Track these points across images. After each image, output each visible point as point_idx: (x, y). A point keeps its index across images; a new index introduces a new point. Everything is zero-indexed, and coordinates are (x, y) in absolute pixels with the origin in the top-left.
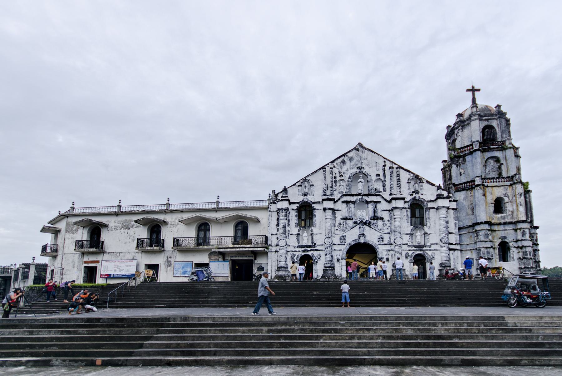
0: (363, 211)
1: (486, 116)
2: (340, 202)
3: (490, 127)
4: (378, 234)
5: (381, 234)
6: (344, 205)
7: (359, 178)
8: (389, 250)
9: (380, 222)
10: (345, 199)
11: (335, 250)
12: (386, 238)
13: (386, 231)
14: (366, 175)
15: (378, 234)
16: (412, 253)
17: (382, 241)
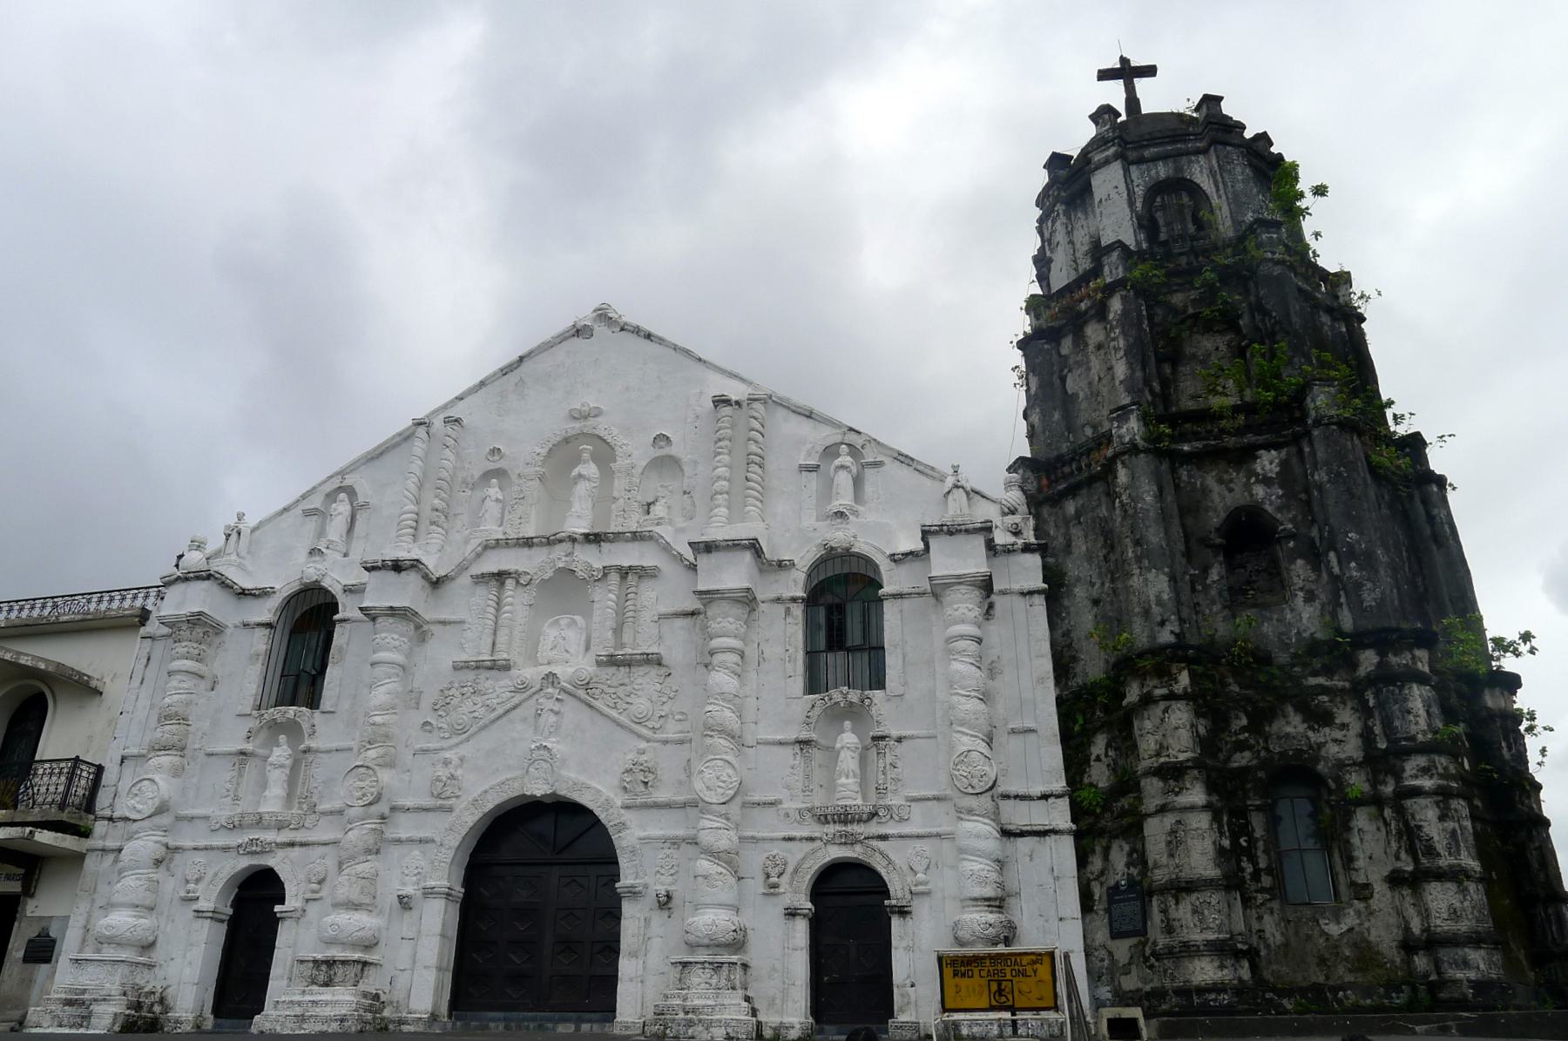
0: (574, 622)
1: (1155, 145)
2: (465, 580)
3: (1181, 185)
4: (628, 751)
5: (643, 745)
6: (484, 596)
7: (577, 460)
8: (675, 842)
9: (646, 680)
10: (492, 564)
11: (399, 841)
12: (668, 764)
13: (672, 731)
14: (604, 452)
15: (628, 751)
16: (800, 856)
17: (646, 783)
